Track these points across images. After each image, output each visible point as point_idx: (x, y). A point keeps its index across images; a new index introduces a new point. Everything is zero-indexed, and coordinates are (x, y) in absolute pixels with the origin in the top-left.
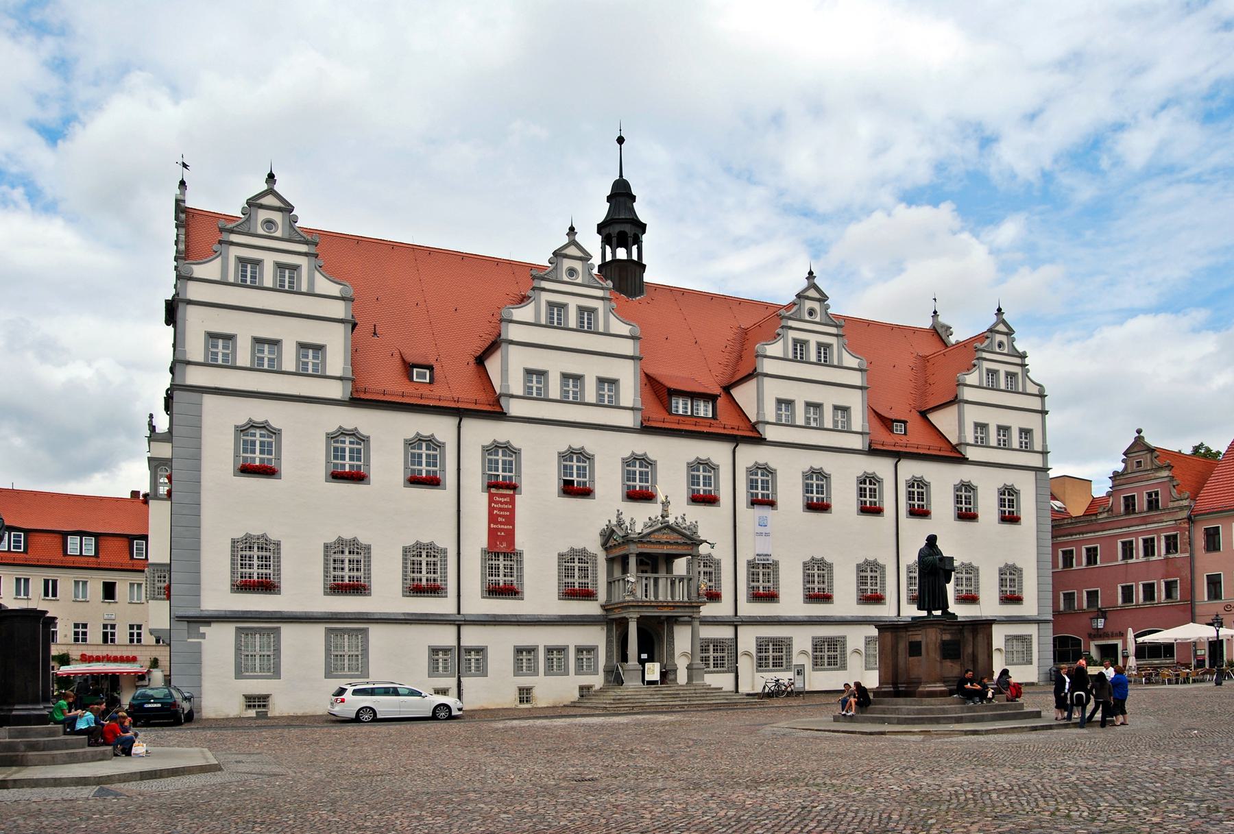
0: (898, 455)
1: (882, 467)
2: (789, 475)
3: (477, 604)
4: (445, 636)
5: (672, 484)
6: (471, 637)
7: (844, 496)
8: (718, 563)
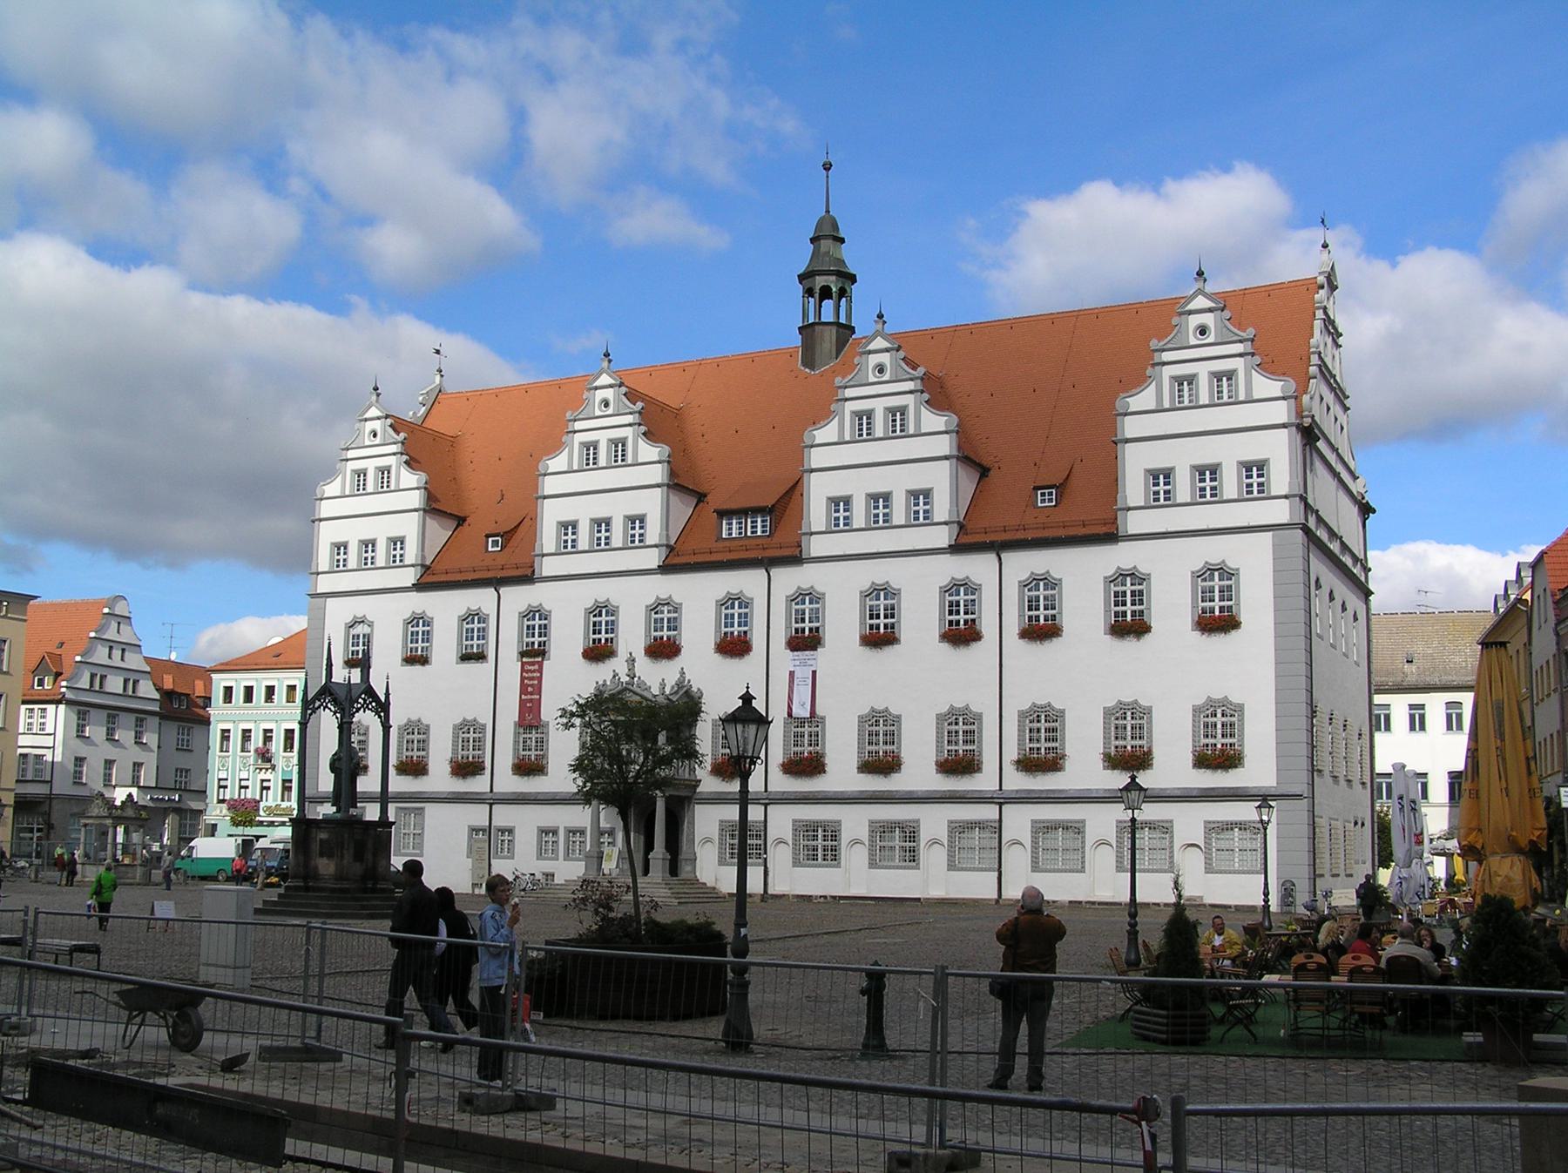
0: (999, 547)
1: (979, 567)
2: (841, 597)
3: (508, 782)
4: (477, 815)
5: (698, 633)
6: (504, 816)
7: (920, 619)
8: (979, 717)
